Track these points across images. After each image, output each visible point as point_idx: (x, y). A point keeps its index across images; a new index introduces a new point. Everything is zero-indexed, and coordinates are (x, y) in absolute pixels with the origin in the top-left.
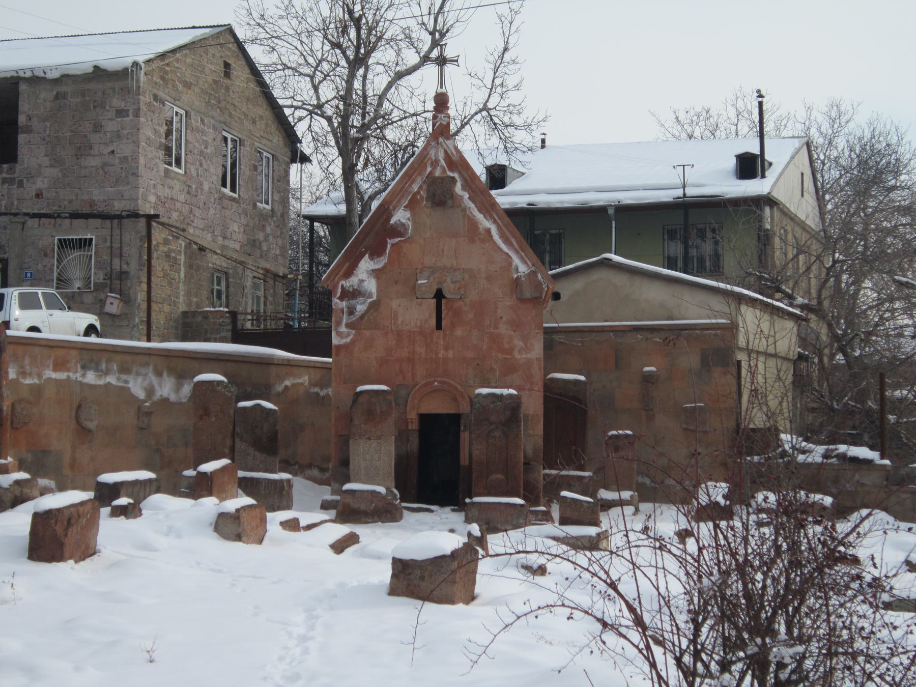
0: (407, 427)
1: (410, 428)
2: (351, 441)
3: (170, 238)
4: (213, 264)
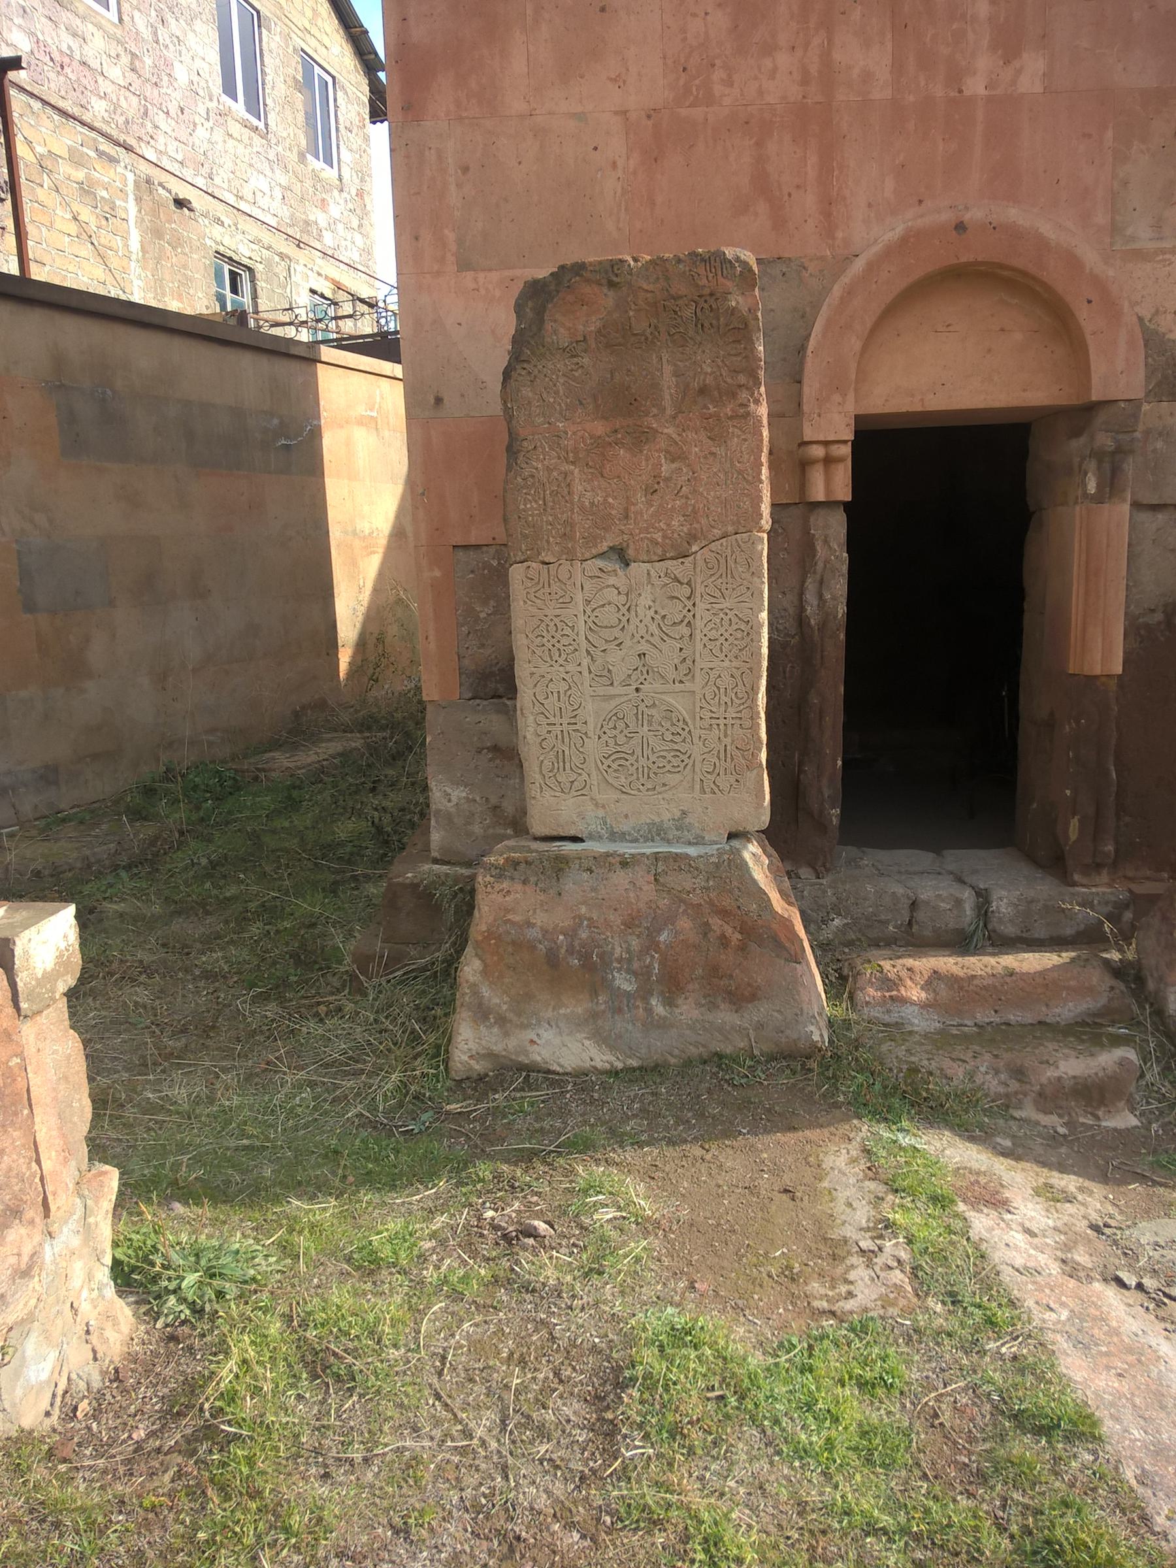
0: (803, 485)
1: (818, 493)
2: (516, 573)
3: (92, 154)
4: (217, 243)
